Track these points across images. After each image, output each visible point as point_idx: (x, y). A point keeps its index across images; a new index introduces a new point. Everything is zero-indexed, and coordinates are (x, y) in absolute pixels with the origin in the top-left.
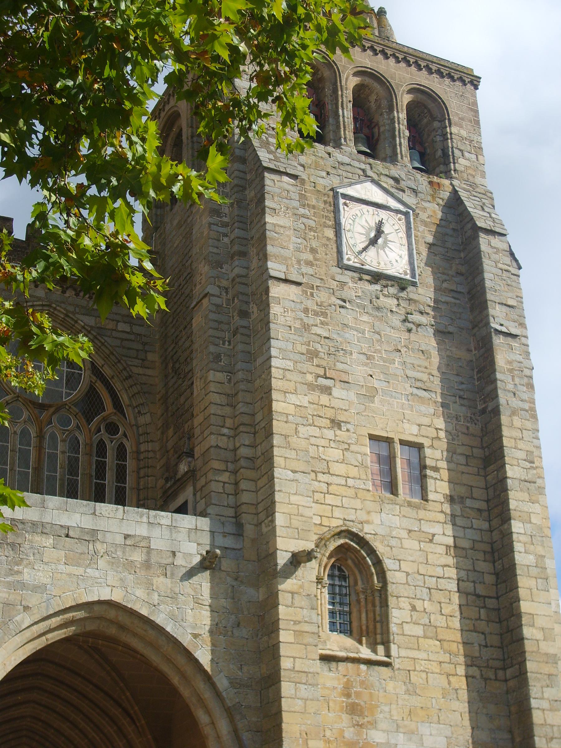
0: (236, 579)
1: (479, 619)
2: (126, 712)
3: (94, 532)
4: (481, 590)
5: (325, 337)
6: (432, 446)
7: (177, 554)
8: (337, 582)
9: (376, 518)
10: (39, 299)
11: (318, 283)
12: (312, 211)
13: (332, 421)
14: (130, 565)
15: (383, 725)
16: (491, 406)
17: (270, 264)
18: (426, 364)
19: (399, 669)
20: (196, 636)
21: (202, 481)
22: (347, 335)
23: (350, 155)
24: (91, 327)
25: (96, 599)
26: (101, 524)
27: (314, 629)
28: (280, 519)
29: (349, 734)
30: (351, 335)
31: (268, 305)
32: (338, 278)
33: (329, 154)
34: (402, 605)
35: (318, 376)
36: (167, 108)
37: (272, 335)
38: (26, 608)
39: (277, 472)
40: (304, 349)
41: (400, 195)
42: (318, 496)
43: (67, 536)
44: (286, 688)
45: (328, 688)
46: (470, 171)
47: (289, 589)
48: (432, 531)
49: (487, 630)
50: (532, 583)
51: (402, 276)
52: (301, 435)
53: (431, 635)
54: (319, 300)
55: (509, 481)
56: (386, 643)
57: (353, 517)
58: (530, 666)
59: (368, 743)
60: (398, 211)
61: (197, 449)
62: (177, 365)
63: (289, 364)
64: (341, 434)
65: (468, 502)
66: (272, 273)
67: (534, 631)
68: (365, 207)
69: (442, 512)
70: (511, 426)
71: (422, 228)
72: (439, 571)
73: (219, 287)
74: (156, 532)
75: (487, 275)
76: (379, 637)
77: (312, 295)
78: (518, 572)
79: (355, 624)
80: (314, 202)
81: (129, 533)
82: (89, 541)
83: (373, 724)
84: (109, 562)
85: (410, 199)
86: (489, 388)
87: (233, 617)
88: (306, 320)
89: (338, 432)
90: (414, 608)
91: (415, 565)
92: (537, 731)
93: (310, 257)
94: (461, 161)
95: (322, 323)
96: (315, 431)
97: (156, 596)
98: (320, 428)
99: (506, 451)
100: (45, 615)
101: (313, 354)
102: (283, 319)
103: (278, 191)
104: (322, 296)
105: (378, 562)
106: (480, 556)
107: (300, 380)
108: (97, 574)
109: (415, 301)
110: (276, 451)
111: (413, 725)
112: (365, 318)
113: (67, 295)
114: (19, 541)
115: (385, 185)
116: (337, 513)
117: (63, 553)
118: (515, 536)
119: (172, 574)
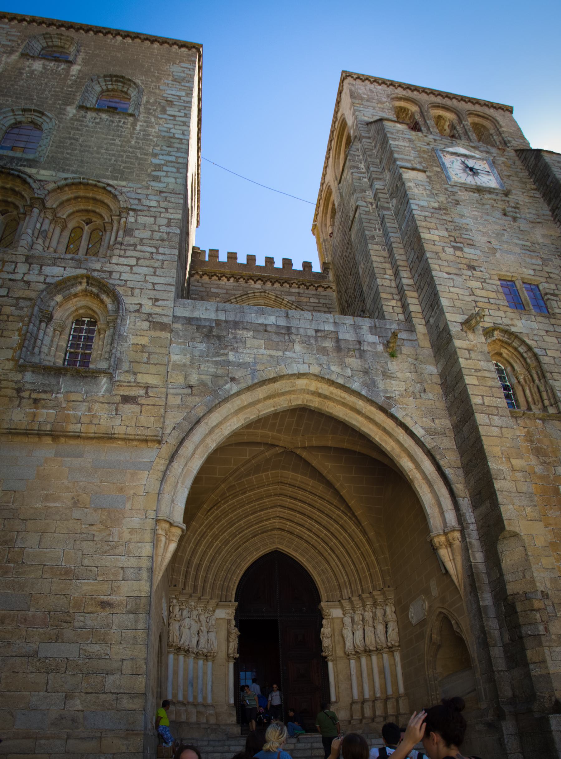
0: (416, 359)
3: (288, 328)
7: (362, 342)
14: (323, 351)
20: (389, 398)
26: (294, 323)
32: (450, 190)
38: (233, 379)
74: (342, 329)
81: (319, 328)
82: (285, 334)
84: (304, 347)
87: (419, 385)
94: (513, 142)
100: (250, 383)
108: (294, 355)
109: (508, 202)
114: (224, 333)
117: (263, 342)
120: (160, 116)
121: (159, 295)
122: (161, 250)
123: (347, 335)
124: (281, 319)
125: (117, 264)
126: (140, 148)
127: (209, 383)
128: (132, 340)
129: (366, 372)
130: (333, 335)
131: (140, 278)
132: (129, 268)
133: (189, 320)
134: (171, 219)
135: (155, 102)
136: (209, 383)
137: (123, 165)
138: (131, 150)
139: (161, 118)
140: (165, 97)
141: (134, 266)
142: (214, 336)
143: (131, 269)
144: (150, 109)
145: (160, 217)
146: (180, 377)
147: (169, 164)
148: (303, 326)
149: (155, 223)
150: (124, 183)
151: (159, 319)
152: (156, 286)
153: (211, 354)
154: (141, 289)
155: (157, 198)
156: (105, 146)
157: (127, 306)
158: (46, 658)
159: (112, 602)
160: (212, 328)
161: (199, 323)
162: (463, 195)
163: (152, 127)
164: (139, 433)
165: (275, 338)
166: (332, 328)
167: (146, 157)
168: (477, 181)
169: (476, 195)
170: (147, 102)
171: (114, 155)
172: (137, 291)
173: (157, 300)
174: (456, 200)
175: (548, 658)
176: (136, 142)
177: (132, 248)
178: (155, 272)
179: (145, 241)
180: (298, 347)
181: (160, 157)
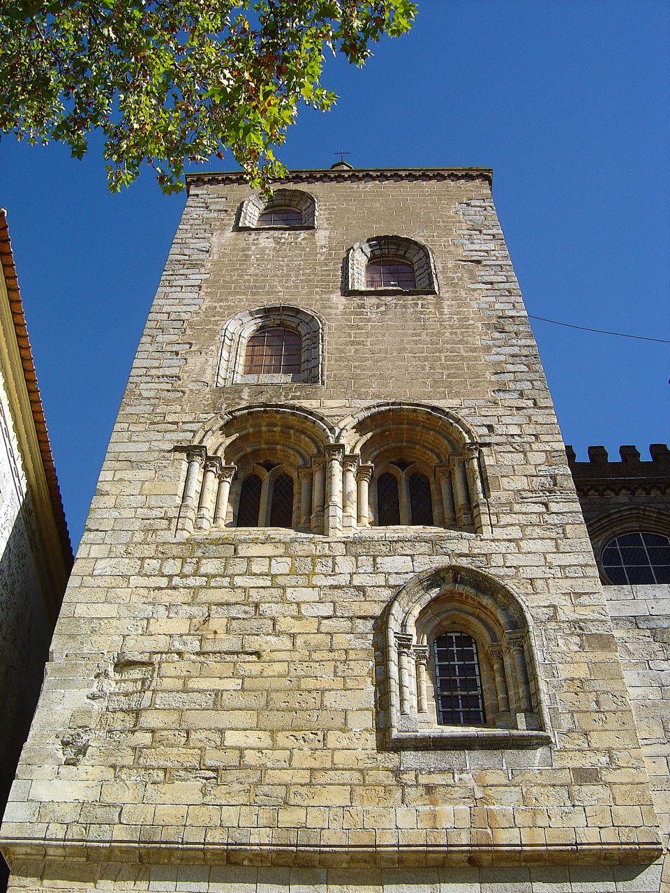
10: (624, 504)
113: (652, 495)
121: (580, 585)
126: (460, 342)
133: (635, 621)
137: (446, 372)
138: (449, 346)
139: (475, 290)
141: (521, 539)
143: (518, 545)
144: (453, 278)
145: (532, 450)
146: (655, 728)
150: (455, 402)
154: (546, 579)
155: (516, 420)
156: (408, 346)
157: (534, 611)
161: (652, 625)
163: (467, 305)
164: (624, 839)
171: (426, 359)
176: (451, 333)
179: (524, 494)
181: (495, 350)
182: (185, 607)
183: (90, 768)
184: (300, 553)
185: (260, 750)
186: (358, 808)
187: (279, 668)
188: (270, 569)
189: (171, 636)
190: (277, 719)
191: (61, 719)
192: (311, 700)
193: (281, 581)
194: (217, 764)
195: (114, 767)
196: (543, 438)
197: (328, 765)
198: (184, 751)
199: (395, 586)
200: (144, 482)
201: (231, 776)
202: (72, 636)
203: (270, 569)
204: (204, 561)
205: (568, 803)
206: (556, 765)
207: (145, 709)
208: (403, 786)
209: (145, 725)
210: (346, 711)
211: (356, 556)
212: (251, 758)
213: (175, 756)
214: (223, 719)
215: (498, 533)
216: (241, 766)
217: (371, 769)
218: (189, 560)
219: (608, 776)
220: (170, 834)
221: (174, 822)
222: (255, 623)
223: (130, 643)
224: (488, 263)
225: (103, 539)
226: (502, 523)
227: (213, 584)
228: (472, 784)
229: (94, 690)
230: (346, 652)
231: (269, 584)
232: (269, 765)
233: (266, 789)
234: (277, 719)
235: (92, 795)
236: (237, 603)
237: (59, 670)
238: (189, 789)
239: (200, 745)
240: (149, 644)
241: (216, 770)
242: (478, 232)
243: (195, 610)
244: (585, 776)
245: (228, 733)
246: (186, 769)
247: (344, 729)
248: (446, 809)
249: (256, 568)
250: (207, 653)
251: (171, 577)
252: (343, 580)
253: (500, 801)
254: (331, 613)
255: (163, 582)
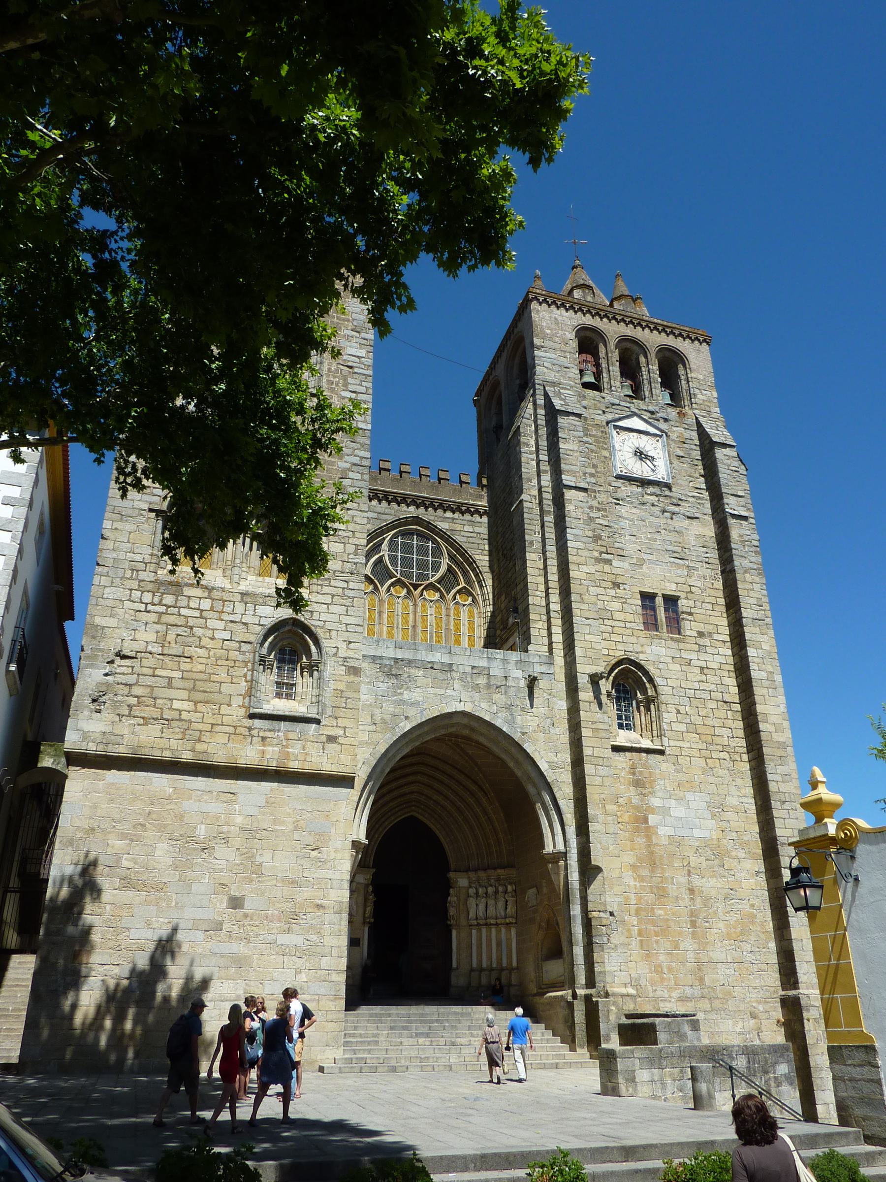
0: (550, 695)
1: (727, 718)
2: (481, 788)
3: (451, 665)
4: (727, 698)
5: (606, 526)
6: (687, 598)
8: (622, 695)
9: (648, 649)
11: (601, 489)
12: (593, 439)
13: (613, 583)
14: (476, 688)
15: (660, 794)
16: (728, 568)
17: (563, 477)
18: (680, 540)
19: (670, 755)
20: (523, 733)
21: (525, 628)
22: (621, 524)
23: (619, 398)
24: (447, 529)
25: (454, 710)
26: (455, 660)
27: (606, 727)
28: (578, 652)
29: (635, 800)
30: (625, 524)
31: (564, 506)
33: (603, 398)
34: (669, 710)
35: (601, 553)
36: (491, 378)
37: (568, 525)
38: (407, 718)
39: (575, 620)
40: (590, 534)
41: (656, 423)
42: (605, 635)
43: (432, 668)
44: (588, 769)
45: (619, 769)
46: (706, 403)
47: (587, 700)
48: (689, 657)
49: (733, 726)
50: (765, 691)
51: (661, 480)
52: (591, 593)
53: (692, 730)
54: (600, 500)
55: (744, 619)
56: (660, 736)
57: (631, 649)
58: (765, 750)
59: (650, 806)
60: (655, 435)
61: (519, 607)
62: (505, 552)
63: (581, 545)
64: (620, 592)
65: (715, 636)
66: (565, 482)
67: (768, 725)
68: (631, 434)
69: (696, 643)
70: (745, 581)
71: (673, 445)
72: (696, 686)
73: (530, 495)
74: (494, 664)
75: (721, 475)
76: (655, 733)
77: (595, 497)
78: (754, 684)
79: (638, 723)
80: (594, 432)
83: (653, 793)
85: (663, 426)
86: (727, 554)
87: (549, 720)
88: (591, 515)
89: (618, 591)
90: (678, 712)
91: (679, 681)
92: (773, 797)
93: (593, 471)
94: (700, 396)
95: (603, 516)
96: (600, 591)
97: (495, 706)
98: (605, 588)
99: (741, 599)
101: (597, 538)
102: (575, 514)
103: (567, 425)
104: (602, 497)
105: (651, 680)
106: (726, 674)
107: (588, 555)
109: (671, 497)
110: (574, 605)
111: (681, 794)
112: (634, 511)
115: (645, 417)
116: (620, 646)
118: (750, 659)
119: (506, 692)
120: (344, 394)
121: (352, 637)
122: (351, 585)
123: (496, 671)
124: (445, 655)
125: (316, 603)
127: (389, 721)
128: (333, 685)
129: (509, 707)
130: (486, 672)
131: (335, 618)
132: (326, 606)
134: (358, 545)
135: (337, 370)
136: (389, 721)
140: (345, 360)
142: (393, 675)
143: (328, 607)
145: (348, 543)
147: (355, 468)
148: (462, 663)
149: (344, 552)
151: (352, 663)
152: (348, 627)
153: (390, 694)
157: (327, 649)
158: (282, 945)
159: (324, 905)
160: (391, 666)
162: (627, 489)
164: (341, 770)
165: (440, 676)
166: (485, 665)
167: (333, 460)
168: (643, 469)
169: (640, 489)
170: (329, 369)
172: (334, 633)
173: (350, 642)
174: (618, 500)
175: (606, 961)
177: (327, 583)
178: (347, 612)
179: (337, 573)
180: (457, 685)
182: (155, 625)
183: (108, 714)
184: (216, 598)
185: (189, 712)
186: (230, 745)
187: (201, 668)
188: (199, 605)
189: (147, 642)
190: (199, 696)
191: (91, 687)
192: (215, 687)
193: (205, 614)
194: (169, 717)
195: (119, 715)
196: (357, 535)
197: (220, 723)
198: (153, 709)
199: (262, 625)
200: (130, 533)
201: (174, 724)
202: (94, 637)
203: (199, 605)
204: (165, 596)
205: (322, 751)
206: (321, 732)
207: (134, 685)
208: (253, 736)
209: (133, 694)
210: (231, 695)
211: (246, 603)
212: (184, 715)
213: (149, 712)
214: (173, 693)
215: (320, 598)
216: (180, 720)
217: (239, 726)
218: (156, 594)
219: (341, 740)
220: (146, 751)
221: (149, 745)
222: (191, 639)
223: (126, 644)
224: (356, 370)
225: (108, 572)
226: (323, 592)
227: (169, 612)
228: (282, 738)
229: (107, 671)
230: (235, 661)
231: (198, 616)
232: (193, 720)
233: (190, 732)
234: (199, 696)
235: (108, 729)
236: (181, 626)
237: (88, 657)
238: (154, 729)
239: (161, 707)
240: (136, 646)
241: (167, 720)
242: (357, 335)
243: (158, 627)
244: (332, 739)
245: (174, 701)
246: (153, 719)
247: (229, 705)
248: (270, 748)
249: (192, 605)
250: (165, 655)
251: (146, 604)
252: (237, 618)
253: (292, 747)
254: (229, 638)
255: (142, 607)
